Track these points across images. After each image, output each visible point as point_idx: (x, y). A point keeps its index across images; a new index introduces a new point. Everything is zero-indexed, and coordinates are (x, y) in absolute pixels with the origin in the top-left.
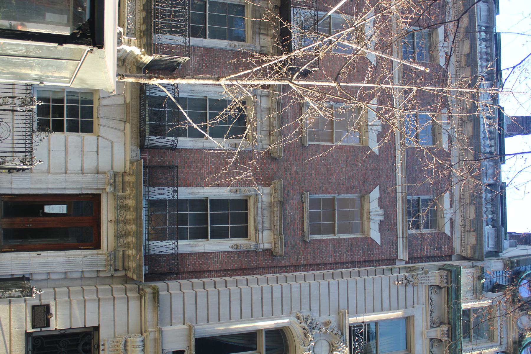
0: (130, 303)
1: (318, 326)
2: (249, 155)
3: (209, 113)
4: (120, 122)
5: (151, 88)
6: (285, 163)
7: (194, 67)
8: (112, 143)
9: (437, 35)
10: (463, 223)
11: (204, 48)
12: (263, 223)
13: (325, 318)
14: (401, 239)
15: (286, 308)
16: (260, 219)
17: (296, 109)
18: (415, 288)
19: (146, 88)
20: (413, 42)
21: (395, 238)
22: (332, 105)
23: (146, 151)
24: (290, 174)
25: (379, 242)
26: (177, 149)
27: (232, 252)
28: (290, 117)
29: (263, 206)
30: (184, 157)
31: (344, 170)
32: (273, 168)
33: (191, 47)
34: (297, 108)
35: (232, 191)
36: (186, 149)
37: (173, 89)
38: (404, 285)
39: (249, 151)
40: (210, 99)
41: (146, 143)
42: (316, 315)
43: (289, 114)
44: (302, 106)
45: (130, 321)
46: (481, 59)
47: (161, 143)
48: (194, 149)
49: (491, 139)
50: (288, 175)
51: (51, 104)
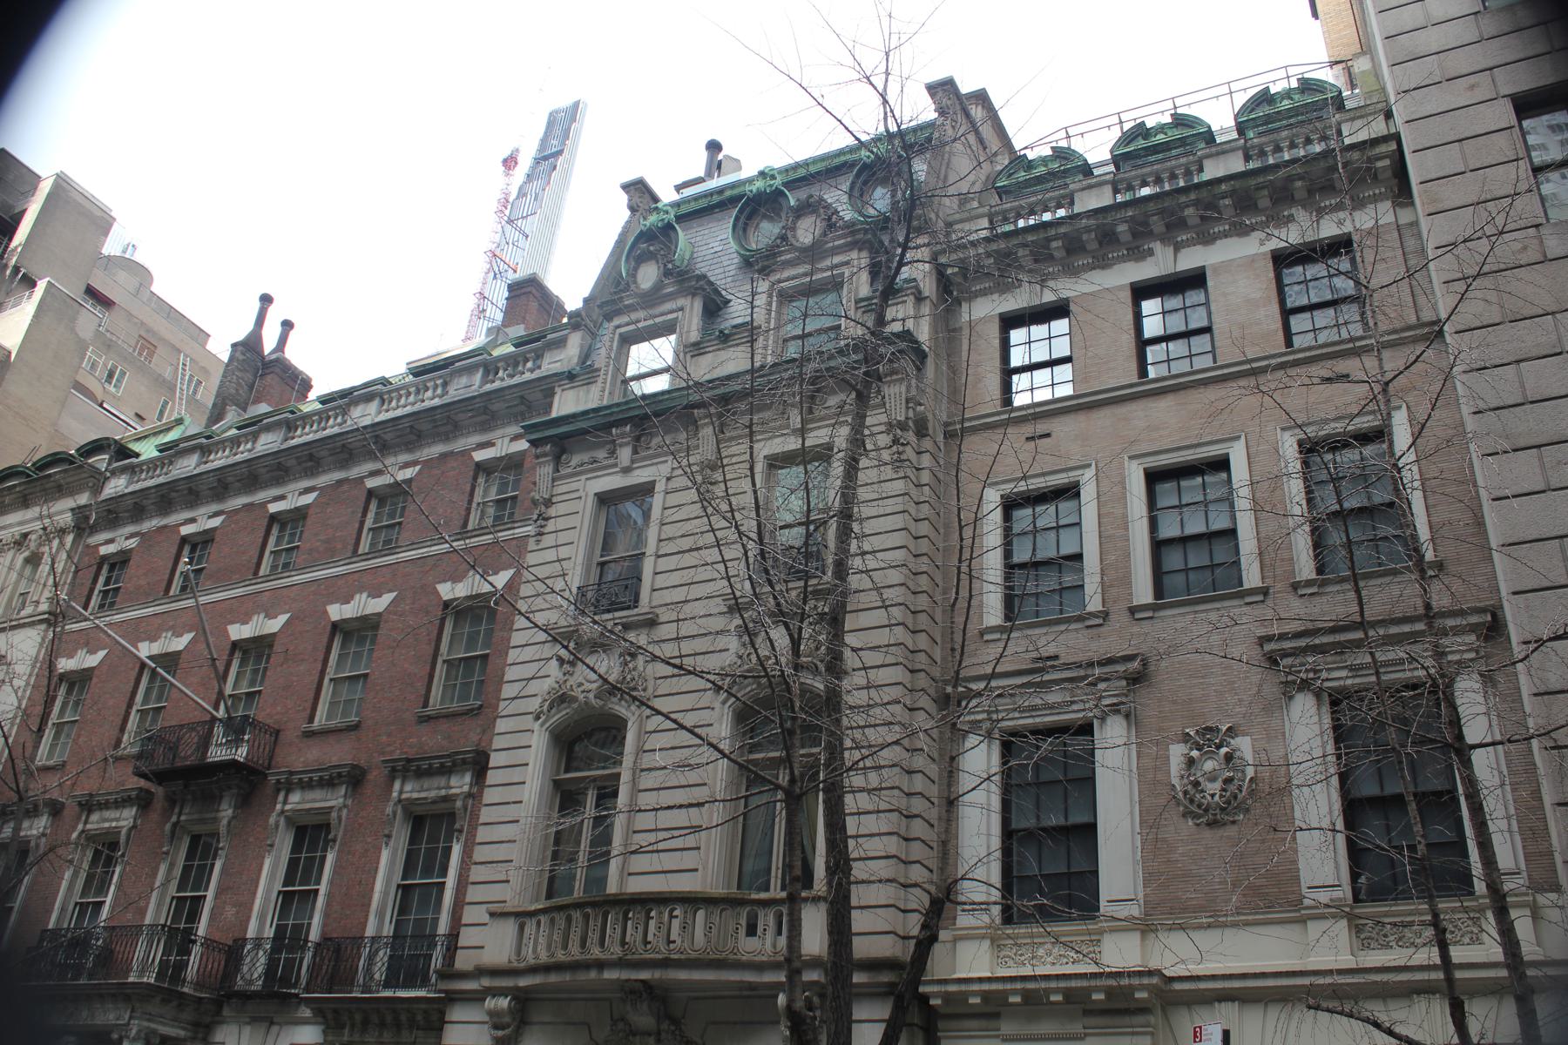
0: (454, 1018)
1: (561, 675)
9: (280, 513)
12: (439, 788)
14: (516, 531)
15: (522, 740)
16: (433, 794)
18: (554, 500)
20: (287, 550)
21: (514, 542)
22: (331, 680)
25: (512, 572)
27: (466, 840)
29: (418, 788)
35: (387, 844)
38: (543, 523)
40: (284, 886)
42: (547, 684)
45: (477, 1019)
46: (324, 429)
49: (427, 389)
50: (388, 749)
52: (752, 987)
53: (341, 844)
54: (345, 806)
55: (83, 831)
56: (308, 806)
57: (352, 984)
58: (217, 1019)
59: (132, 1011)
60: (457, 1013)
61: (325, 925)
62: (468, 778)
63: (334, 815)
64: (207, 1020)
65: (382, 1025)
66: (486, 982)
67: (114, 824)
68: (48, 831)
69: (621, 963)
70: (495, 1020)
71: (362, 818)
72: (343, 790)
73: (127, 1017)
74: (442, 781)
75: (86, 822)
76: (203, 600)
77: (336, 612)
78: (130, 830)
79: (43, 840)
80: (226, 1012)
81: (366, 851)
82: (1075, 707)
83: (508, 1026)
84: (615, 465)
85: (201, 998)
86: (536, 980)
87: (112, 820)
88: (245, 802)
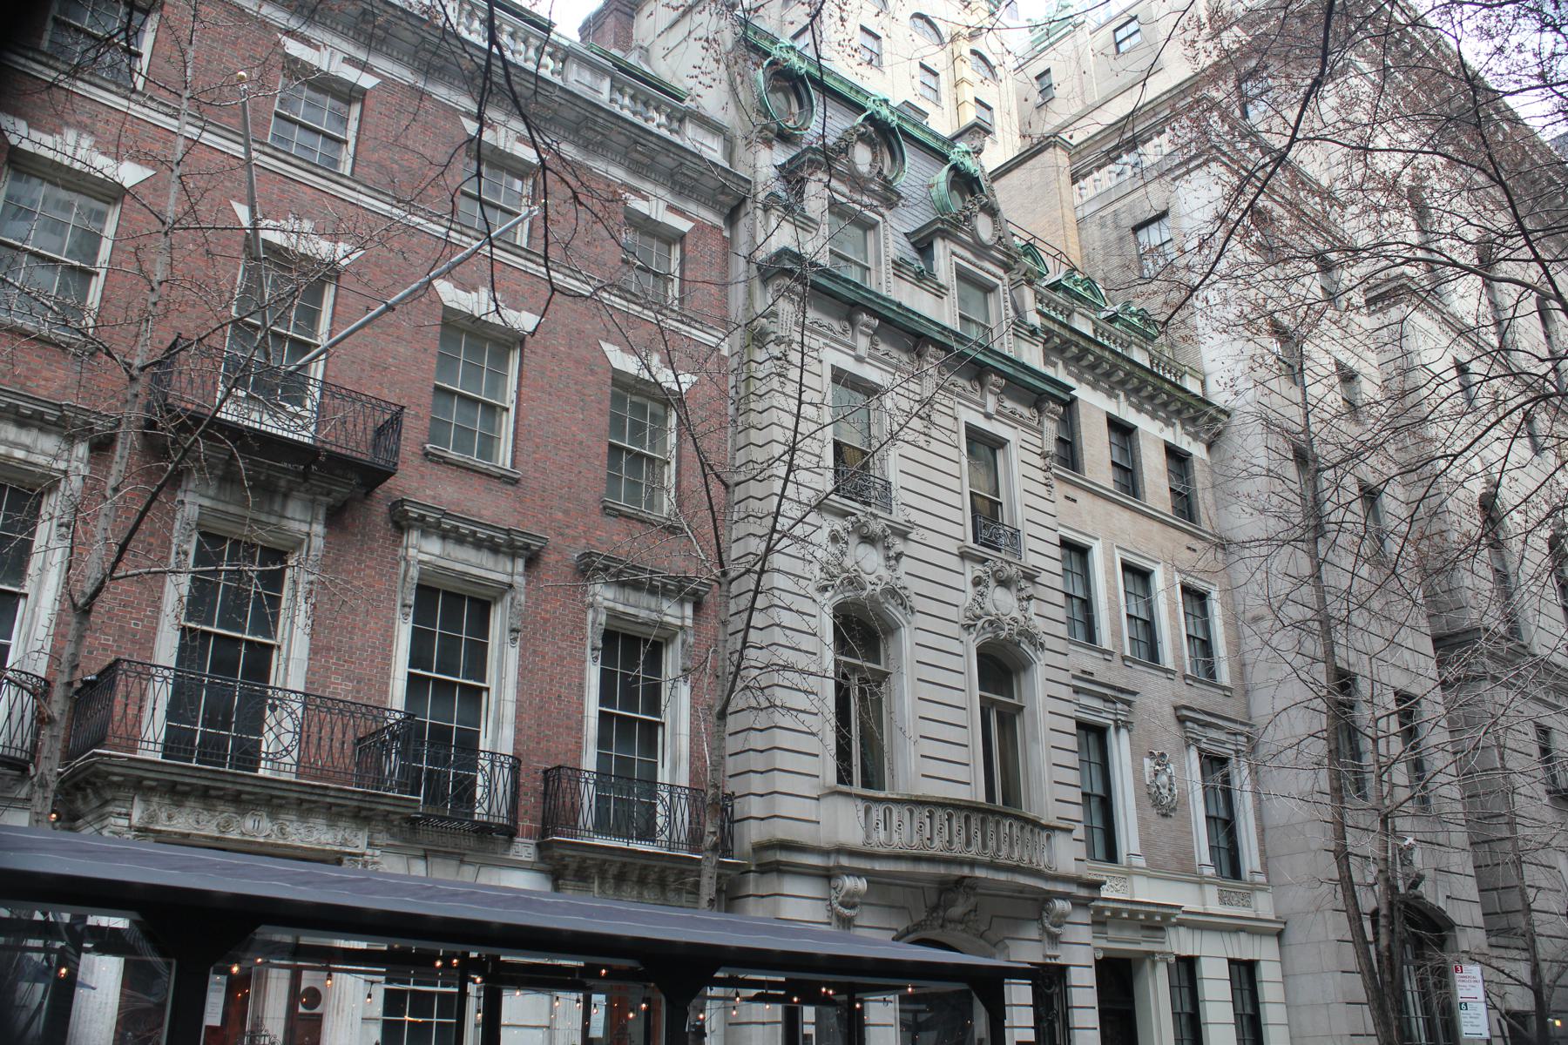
3: (437, 672)
7: (351, 691)
10: (677, 188)
11: (310, 659)
13: (822, 536)
14: (693, 331)
16: (643, 614)
24: (568, 527)
31: (568, 408)
33: (306, 688)
43: (456, 495)
51: (435, 1020)
52: (1023, 889)
56: (459, 567)
57: (575, 827)
60: (791, 885)
61: (516, 742)
62: (688, 610)
65: (642, 882)
66: (845, 861)
67: (19, 454)
69: (993, 866)
70: (847, 899)
71: (546, 611)
74: (653, 602)
76: (208, 138)
77: (447, 291)
81: (562, 658)
82: (1104, 715)
83: (852, 906)
84: (854, 349)
86: (903, 867)
87: (16, 445)
88: (336, 518)
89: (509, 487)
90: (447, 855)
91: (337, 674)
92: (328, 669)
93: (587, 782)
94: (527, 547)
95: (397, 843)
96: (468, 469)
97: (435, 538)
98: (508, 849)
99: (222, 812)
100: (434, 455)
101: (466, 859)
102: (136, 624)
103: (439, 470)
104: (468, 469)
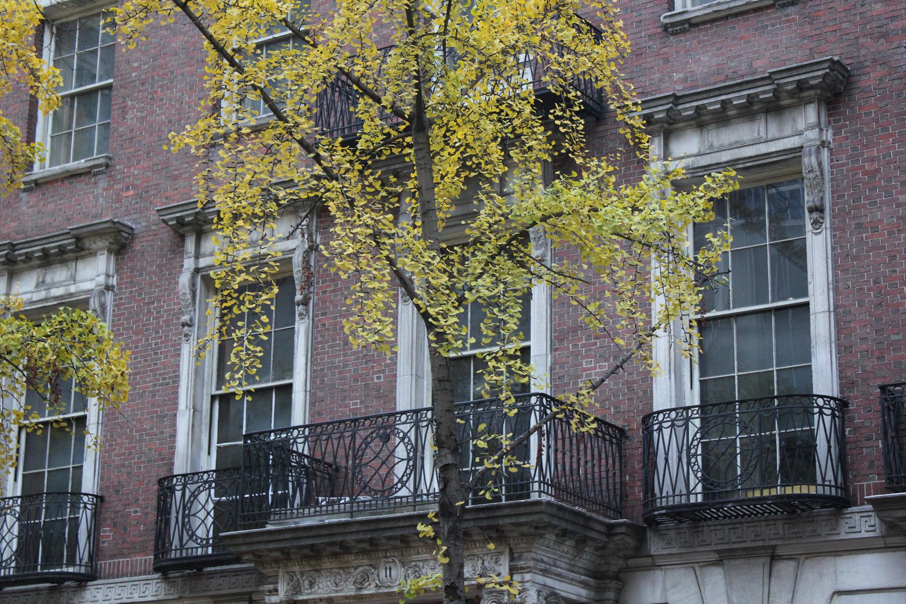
2: (843, 165)
4: (774, 574)
5: (674, 490)
6: (861, 41)
8: (839, 593)
11: (553, 349)
17: (699, 43)
19: (662, 508)
23: (855, 490)
24: (893, 18)
26: (842, 391)
28: (723, 54)
30: (864, 367)
32: (881, 80)
34: (694, 38)
36: (840, 365)
37: (672, 426)
39: (831, 167)
41: (827, 492)
43: (714, 61)
44: (687, 26)
47: (829, 447)
48: (838, 338)
53: (833, 217)
54: (823, 144)
55: (197, 270)
58: (632, 562)
59: (512, 559)
61: (842, 369)
63: (809, 161)
64: (616, 564)
68: (114, 281)
71: (872, 160)
72: (811, 114)
73: (504, 569)
75: (197, 256)
78: (307, 253)
79: (109, 297)
80: (655, 547)
85: (611, 527)
89: (791, 9)
90: (749, 553)
91: (588, 357)
92: (577, 355)
93: (821, 413)
94: (801, 86)
95: (674, 551)
96: (726, 18)
97: (689, 132)
98: (834, 529)
99: (356, 568)
100: (673, 25)
101: (780, 552)
102: (379, 378)
103: (687, 41)
104: (726, 18)
